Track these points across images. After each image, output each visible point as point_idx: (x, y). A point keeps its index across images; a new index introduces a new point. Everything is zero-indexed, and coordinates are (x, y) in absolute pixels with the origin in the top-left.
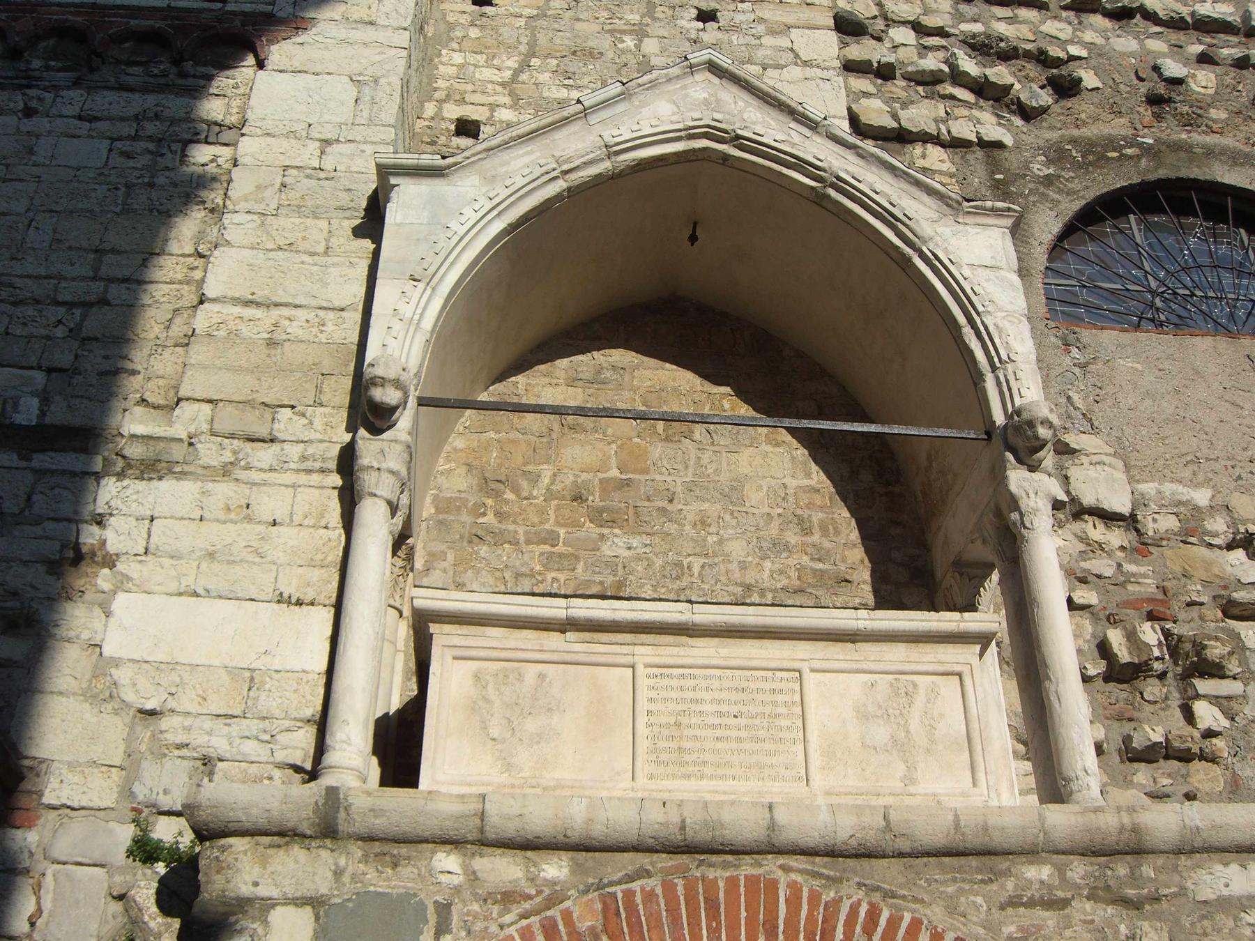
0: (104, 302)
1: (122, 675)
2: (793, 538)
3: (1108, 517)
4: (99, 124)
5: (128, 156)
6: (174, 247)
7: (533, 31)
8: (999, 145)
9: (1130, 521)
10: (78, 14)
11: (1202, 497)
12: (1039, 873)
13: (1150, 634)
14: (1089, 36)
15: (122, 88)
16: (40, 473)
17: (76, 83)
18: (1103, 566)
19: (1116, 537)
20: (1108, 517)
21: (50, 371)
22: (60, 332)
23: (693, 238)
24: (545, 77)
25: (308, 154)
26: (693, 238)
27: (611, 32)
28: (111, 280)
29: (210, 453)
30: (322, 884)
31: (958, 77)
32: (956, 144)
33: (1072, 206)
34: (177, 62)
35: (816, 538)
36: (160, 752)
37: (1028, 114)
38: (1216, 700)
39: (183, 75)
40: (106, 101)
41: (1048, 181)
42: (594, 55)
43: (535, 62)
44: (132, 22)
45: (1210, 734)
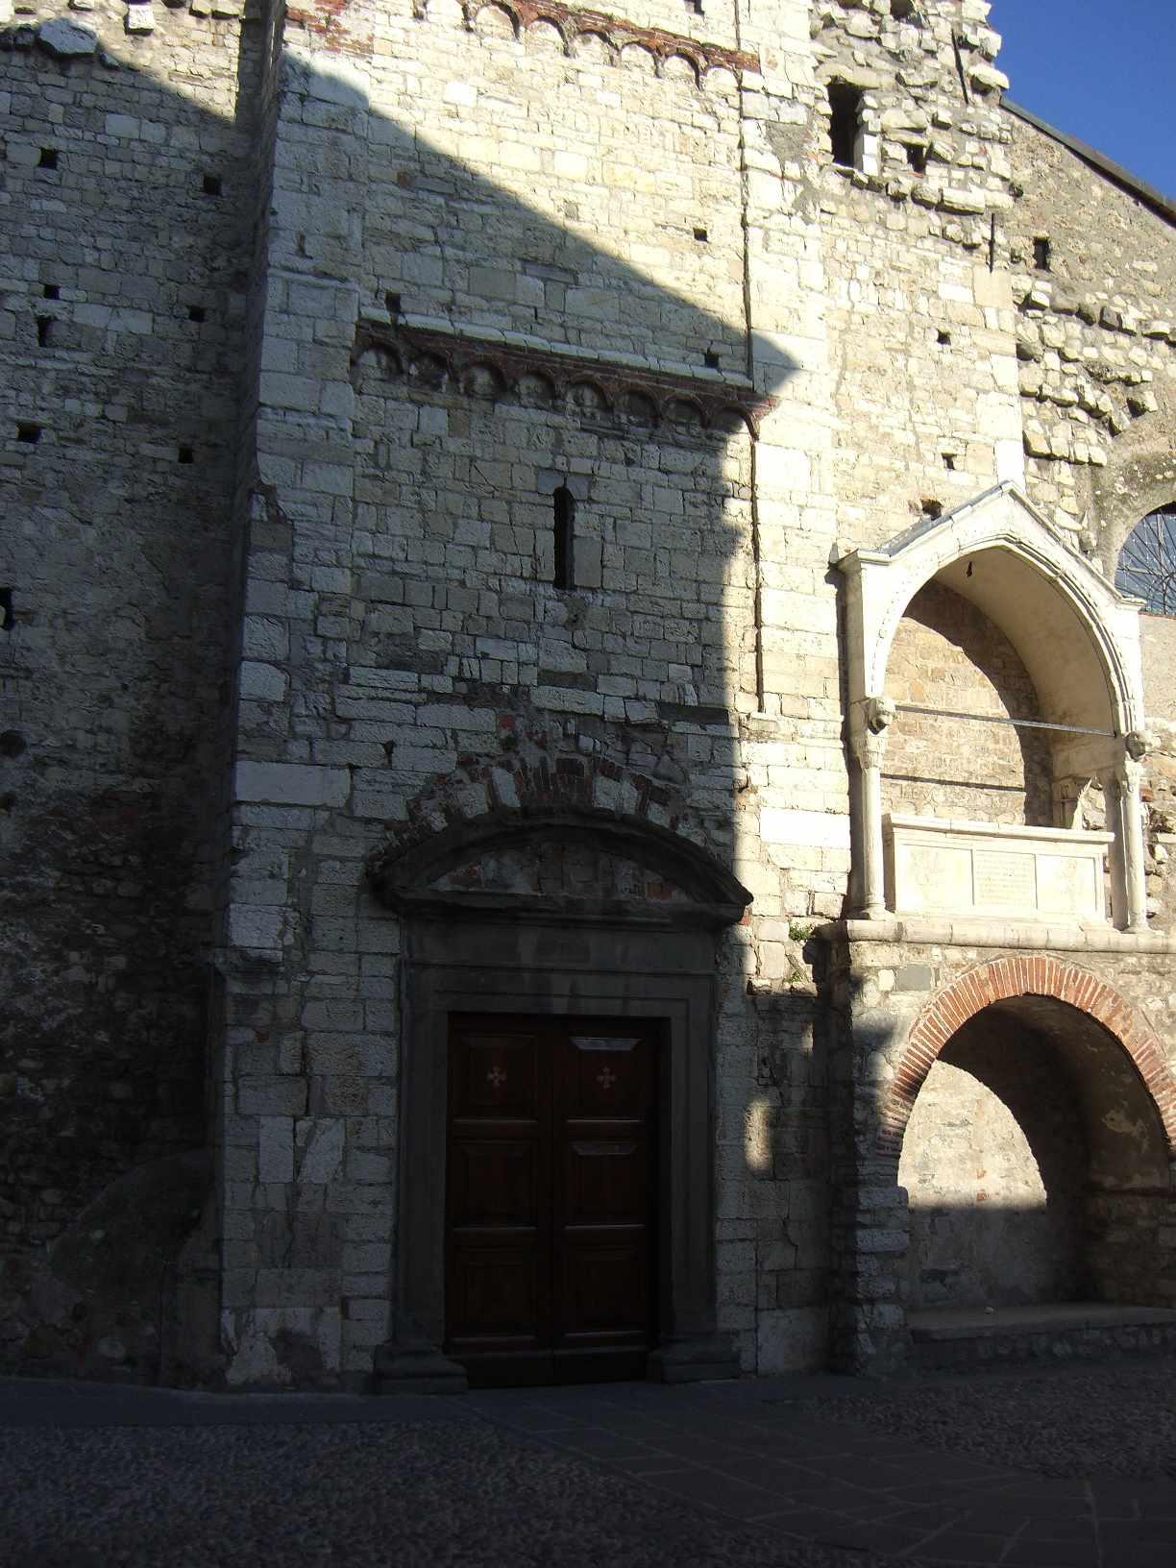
0: (708, 619)
1: (771, 850)
2: (991, 746)
4: (675, 478)
5: (695, 506)
6: (734, 581)
7: (843, 342)
8: (1100, 466)
10: (641, 378)
12: (1132, 960)
14: (1156, 362)
15: (678, 445)
16: (713, 737)
17: (651, 439)
21: (693, 666)
22: (691, 639)
23: (970, 573)
24: (854, 391)
26: (970, 573)
27: (889, 349)
28: (708, 604)
29: (786, 727)
30: (896, 961)
31: (1082, 404)
34: (705, 424)
35: (1001, 746)
36: (792, 888)
38: (1165, 845)
39: (710, 437)
41: (1124, 499)
42: (882, 372)
43: (848, 375)
44: (678, 390)
45: (1160, 863)
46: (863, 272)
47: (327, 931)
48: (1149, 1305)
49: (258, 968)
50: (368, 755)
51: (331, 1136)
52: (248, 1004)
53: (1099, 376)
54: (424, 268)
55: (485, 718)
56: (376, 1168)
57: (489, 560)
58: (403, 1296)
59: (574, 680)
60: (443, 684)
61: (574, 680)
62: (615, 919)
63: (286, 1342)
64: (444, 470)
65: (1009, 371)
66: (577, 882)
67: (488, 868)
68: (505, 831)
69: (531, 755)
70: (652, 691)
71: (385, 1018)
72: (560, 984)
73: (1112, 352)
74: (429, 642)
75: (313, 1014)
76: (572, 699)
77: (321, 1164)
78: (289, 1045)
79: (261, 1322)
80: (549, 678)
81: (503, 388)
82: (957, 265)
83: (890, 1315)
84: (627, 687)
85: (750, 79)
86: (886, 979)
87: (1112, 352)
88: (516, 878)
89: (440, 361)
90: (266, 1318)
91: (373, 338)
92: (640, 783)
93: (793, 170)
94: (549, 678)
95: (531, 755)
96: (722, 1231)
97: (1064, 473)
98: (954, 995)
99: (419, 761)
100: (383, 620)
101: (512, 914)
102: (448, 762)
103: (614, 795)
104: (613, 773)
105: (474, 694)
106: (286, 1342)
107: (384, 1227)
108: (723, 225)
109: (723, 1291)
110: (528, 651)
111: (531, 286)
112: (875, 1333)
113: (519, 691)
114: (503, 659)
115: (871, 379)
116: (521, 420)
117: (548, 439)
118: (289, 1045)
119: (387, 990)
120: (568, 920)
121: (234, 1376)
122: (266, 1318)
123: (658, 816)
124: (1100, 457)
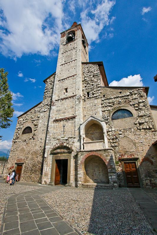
3: (113, 131)
9: (115, 131)
11: (118, 129)
13: (114, 137)
18: (113, 133)
19: (114, 132)
20: (113, 131)
25: (78, 123)
31: (108, 106)
32: (107, 110)
33: (113, 113)
37: (112, 107)
40: (71, 122)
41: (112, 112)
46: (89, 104)
47: (49, 155)
48: (93, 185)
49: (46, 158)
50: (51, 144)
51: (48, 168)
52: (45, 160)
53: (109, 103)
54: (58, 116)
55: (58, 141)
56: (50, 170)
57: (59, 131)
58: (51, 178)
59: (63, 137)
60: (56, 139)
61: (63, 137)
62: (64, 153)
63: (45, 181)
64: (57, 127)
65: (101, 106)
66: (62, 150)
67: (57, 150)
68: (58, 148)
69: (60, 142)
70: (68, 137)
71: (51, 160)
72: (61, 157)
73: (111, 101)
74: (55, 137)
75: (48, 160)
76: (64, 138)
77: (47, 170)
78: (47, 162)
79: (44, 179)
80: (62, 138)
81: (61, 121)
82: (96, 100)
83: (80, 183)
84: (66, 137)
85: (76, 96)
86: (80, 155)
87: (111, 101)
88: (59, 151)
89: (58, 121)
90: (44, 180)
91: (54, 121)
92: (67, 143)
93: (79, 100)
94: (62, 138)
95: (60, 142)
96: (71, 175)
97: (106, 111)
98: (86, 156)
99: (54, 144)
100: (53, 136)
101: (58, 153)
102: (56, 144)
103: (65, 144)
104: (65, 143)
105: (58, 139)
106: (45, 181)
107: (50, 174)
108: (74, 106)
109: (71, 180)
110: (61, 136)
111: (63, 114)
112: (79, 184)
113: (60, 139)
114: (59, 137)
115: (89, 111)
116: (62, 122)
117: (63, 123)
118: (47, 162)
119: (51, 158)
120: (61, 153)
121: (42, 184)
122: (44, 180)
123: (68, 146)
124: (110, 109)
